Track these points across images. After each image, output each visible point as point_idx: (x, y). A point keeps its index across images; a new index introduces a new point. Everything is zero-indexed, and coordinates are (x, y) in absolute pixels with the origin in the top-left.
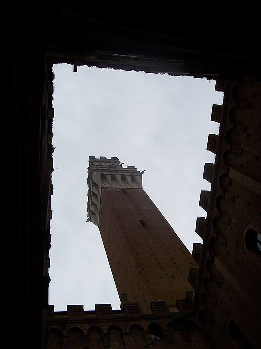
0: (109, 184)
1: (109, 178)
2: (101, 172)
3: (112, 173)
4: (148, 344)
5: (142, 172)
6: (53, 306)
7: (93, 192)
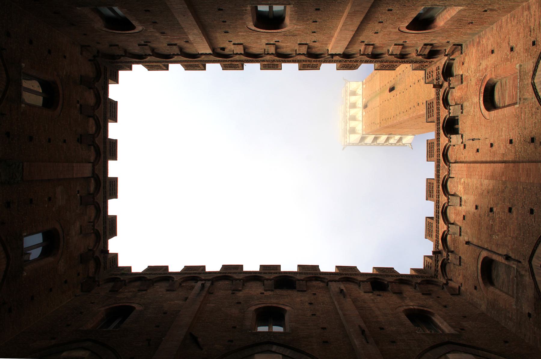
2: (348, 133)
3: (348, 120)
4: (462, 143)
7: (373, 142)
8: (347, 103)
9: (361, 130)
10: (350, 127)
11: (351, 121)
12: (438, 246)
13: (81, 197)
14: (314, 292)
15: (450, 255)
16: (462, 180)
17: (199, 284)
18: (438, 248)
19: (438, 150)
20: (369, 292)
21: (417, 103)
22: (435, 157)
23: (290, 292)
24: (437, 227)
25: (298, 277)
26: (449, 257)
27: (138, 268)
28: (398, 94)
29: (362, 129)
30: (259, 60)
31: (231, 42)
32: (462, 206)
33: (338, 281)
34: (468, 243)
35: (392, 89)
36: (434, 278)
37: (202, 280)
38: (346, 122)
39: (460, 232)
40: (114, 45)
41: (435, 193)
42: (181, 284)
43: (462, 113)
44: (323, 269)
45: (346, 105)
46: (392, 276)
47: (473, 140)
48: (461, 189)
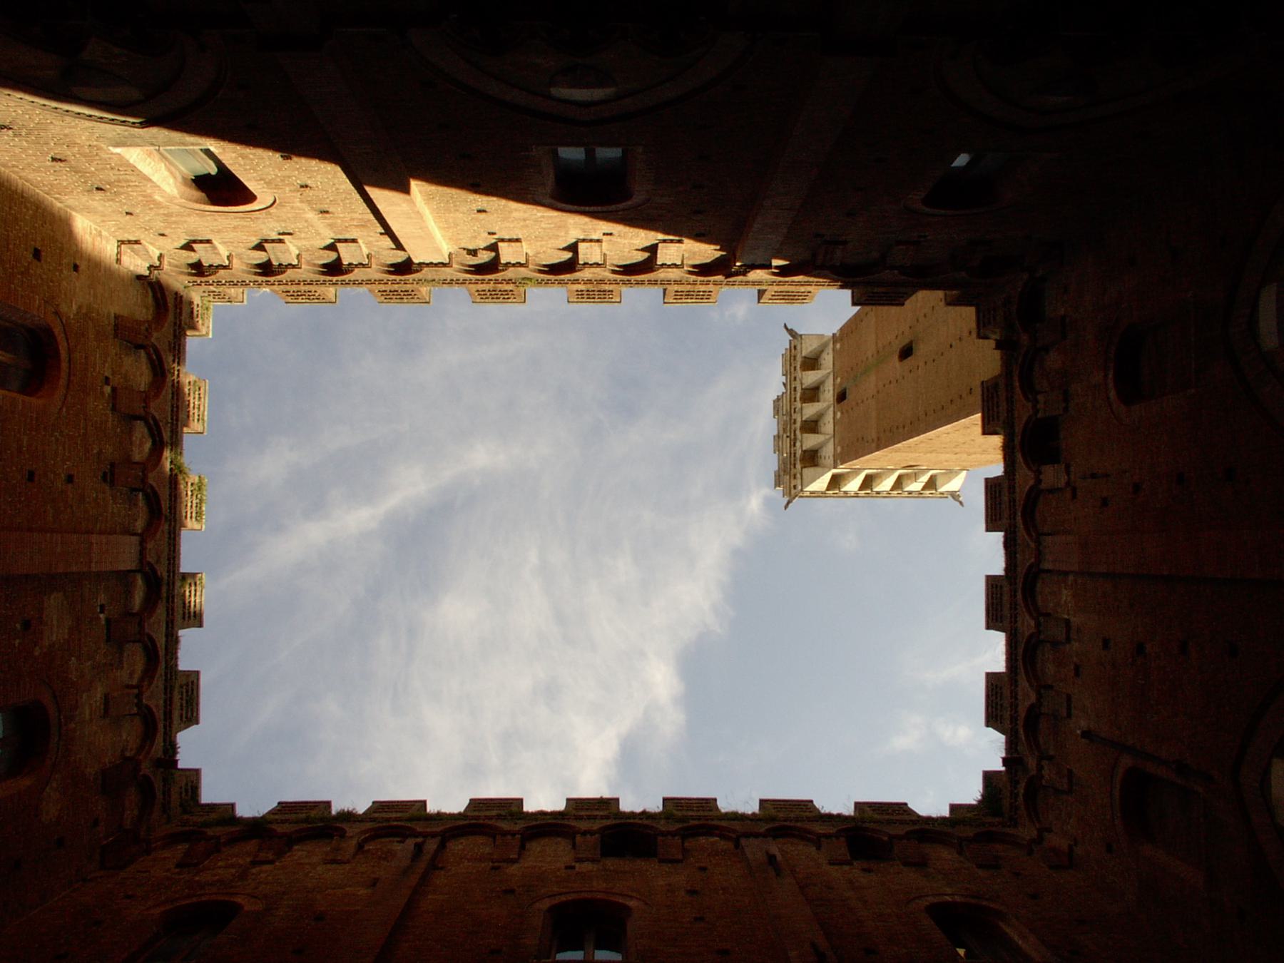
0: (824, 440)
1: (810, 441)
2: (799, 466)
3: (798, 432)
4: (1068, 484)
5: (792, 333)
6: (989, 777)
7: (861, 488)
8: (795, 388)
9: (832, 458)
10: (804, 448)
11: (805, 435)
12: (1017, 745)
13: (108, 620)
14: (702, 865)
15: (1046, 768)
16: (1071, 578)
17: (410, 842)
18: (1016, 750)
19: (1012, 501)
20: (841, 863)
21: (969, 388)
22: (1005, 521)
23: (641, 864)
24: (1014, 695)
25: (662, 826)
26: (1043, 772)
27: (251, 806)
28: (922, 364)
29: (834, 456)
30: (563, 280)
31: (494, 234)
32: (1073, 642)
33: (765, 835)
34: (1086, 734)
35: (906, 352)
36: (1009, 827)
37: (416, 835)
38: (793, 437)
39: (1069, 708)
40: (201, 242)
41: (1006, 612)
42: (363, 847)
43: (1066, 409)
44: (725, 806)
45: (793, 392)
46: (902, 822)
47: (1093, 476)
48: (1069, 599)
